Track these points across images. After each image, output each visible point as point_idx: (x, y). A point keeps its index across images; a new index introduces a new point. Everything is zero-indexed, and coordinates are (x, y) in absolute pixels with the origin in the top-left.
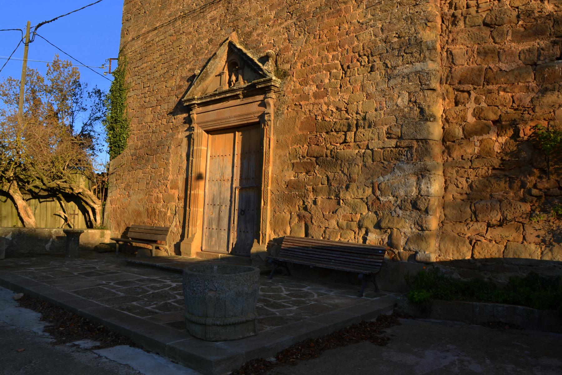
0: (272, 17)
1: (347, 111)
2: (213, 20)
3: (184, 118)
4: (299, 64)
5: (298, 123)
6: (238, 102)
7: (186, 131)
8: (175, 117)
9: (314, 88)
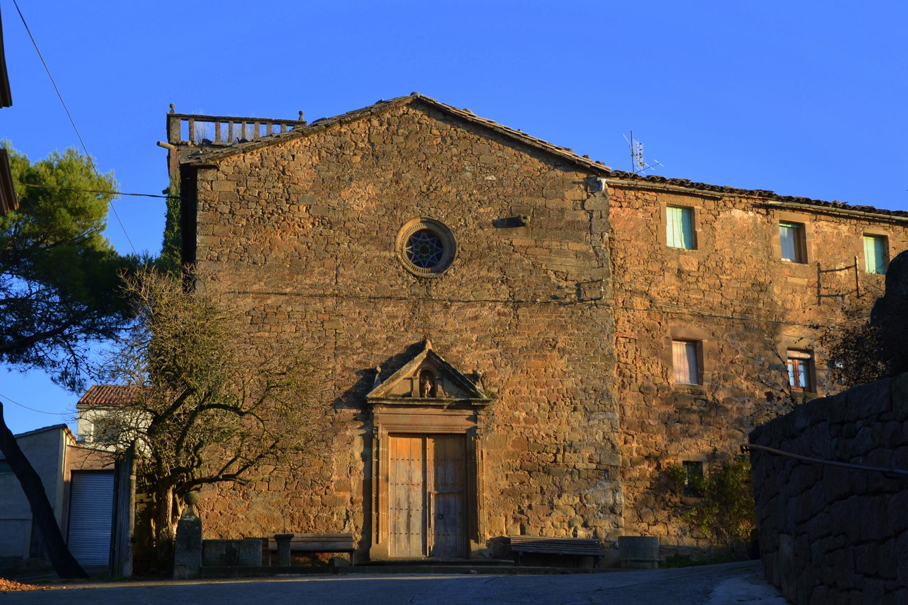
0: (474, 339)
1: (556, 438)
2: (392, 317)
3: (354, 415)
4: (507, 391)
5: (510, 441)
6: (440, 411)
7: (359, 428)
8: (339, 410)
9: (524, 414)
